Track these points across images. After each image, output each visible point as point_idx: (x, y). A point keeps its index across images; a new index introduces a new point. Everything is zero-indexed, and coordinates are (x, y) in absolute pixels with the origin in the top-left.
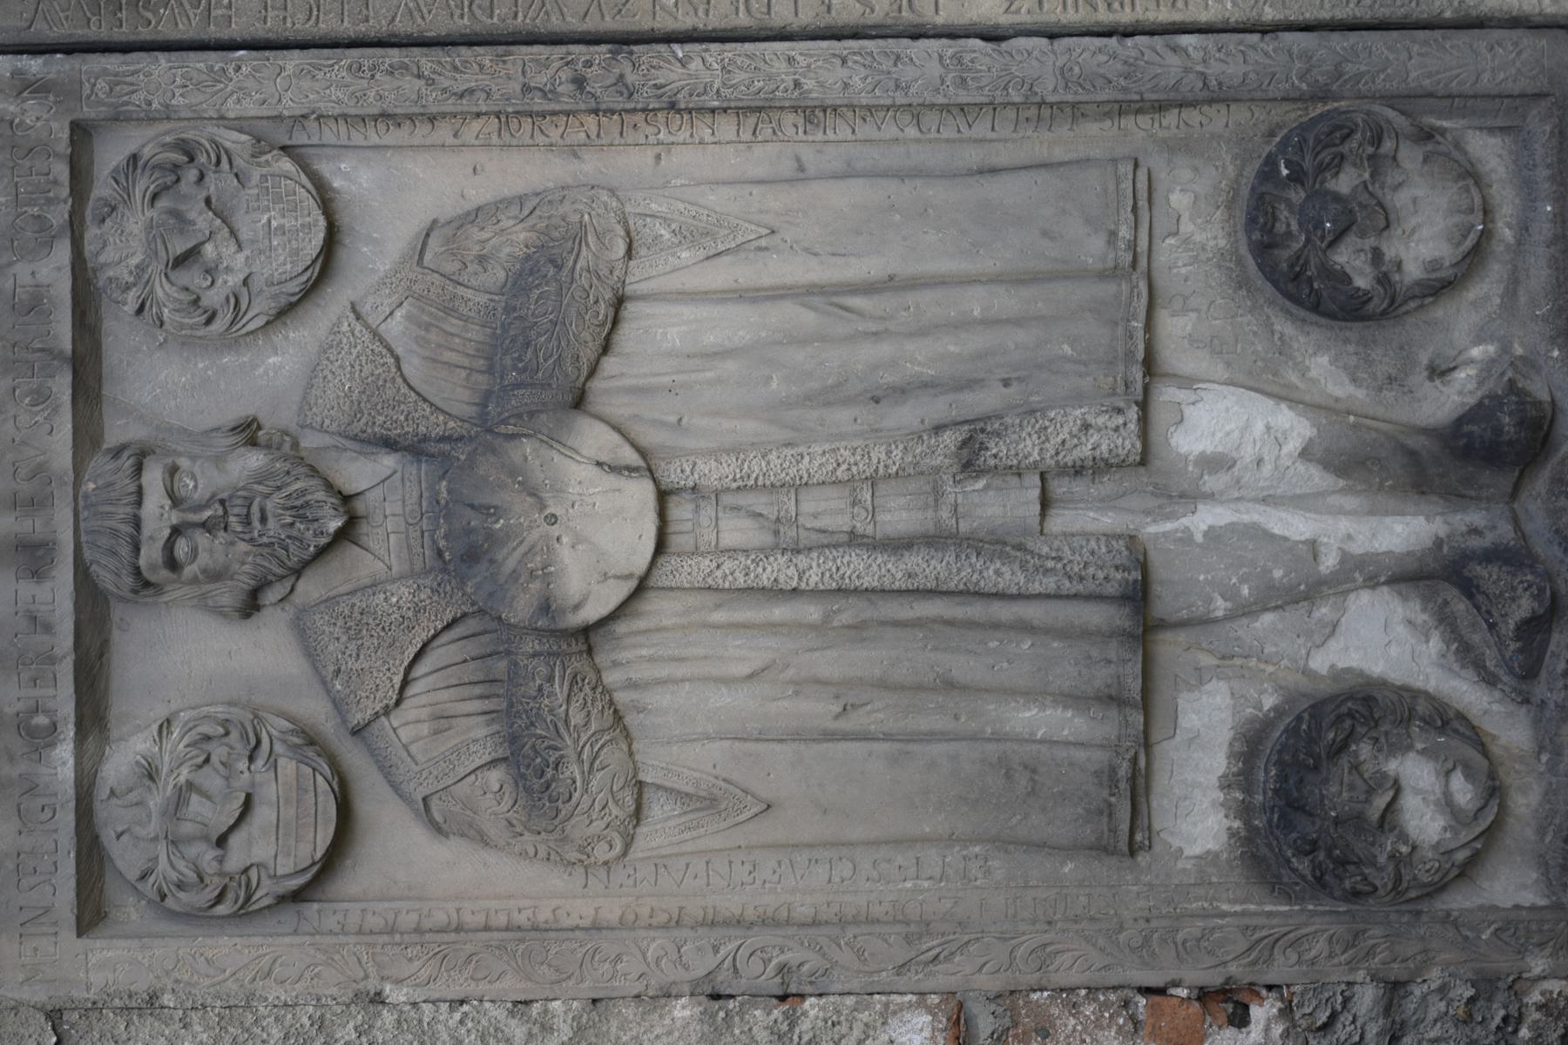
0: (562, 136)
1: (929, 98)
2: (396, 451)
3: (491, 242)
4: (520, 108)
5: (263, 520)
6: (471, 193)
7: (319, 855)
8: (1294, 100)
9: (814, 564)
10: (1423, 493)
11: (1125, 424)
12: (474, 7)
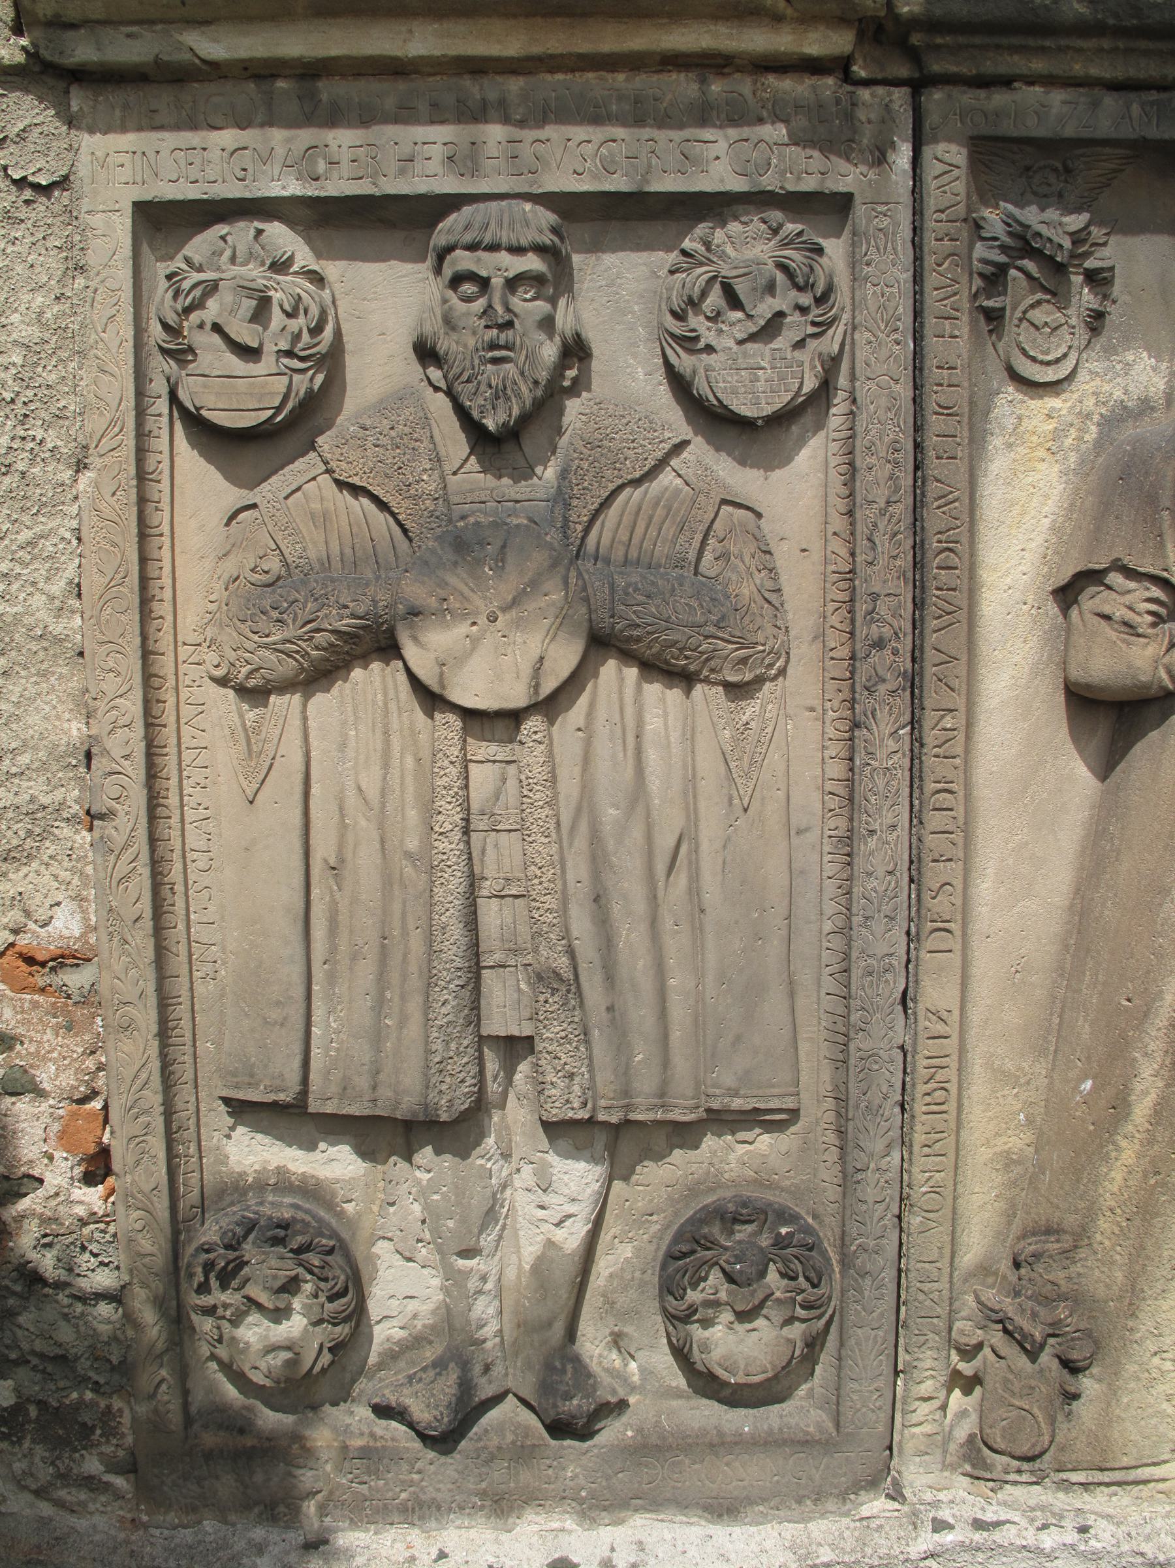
0: (832, 627)
1: (857, 944)
2: (557, 479)
3: (741, 564)
4: (858, 591)
5: (495, 361)
6: (785, 546)
7: (203, 412)
8: (843, 1239)
9: (453, 846)
10: (519, 1326)
11: (573, 1109)
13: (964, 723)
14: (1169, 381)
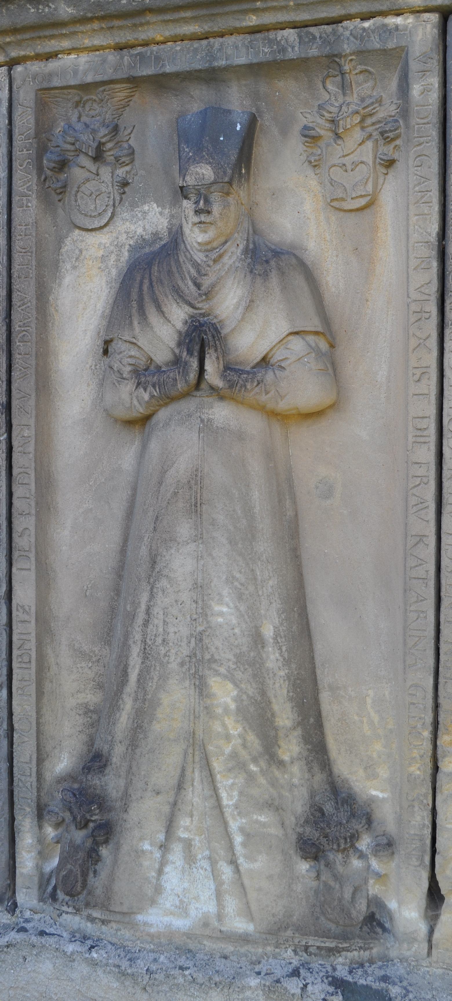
12: (25, 333)
13: (34, 433)
14: (170, 220)
